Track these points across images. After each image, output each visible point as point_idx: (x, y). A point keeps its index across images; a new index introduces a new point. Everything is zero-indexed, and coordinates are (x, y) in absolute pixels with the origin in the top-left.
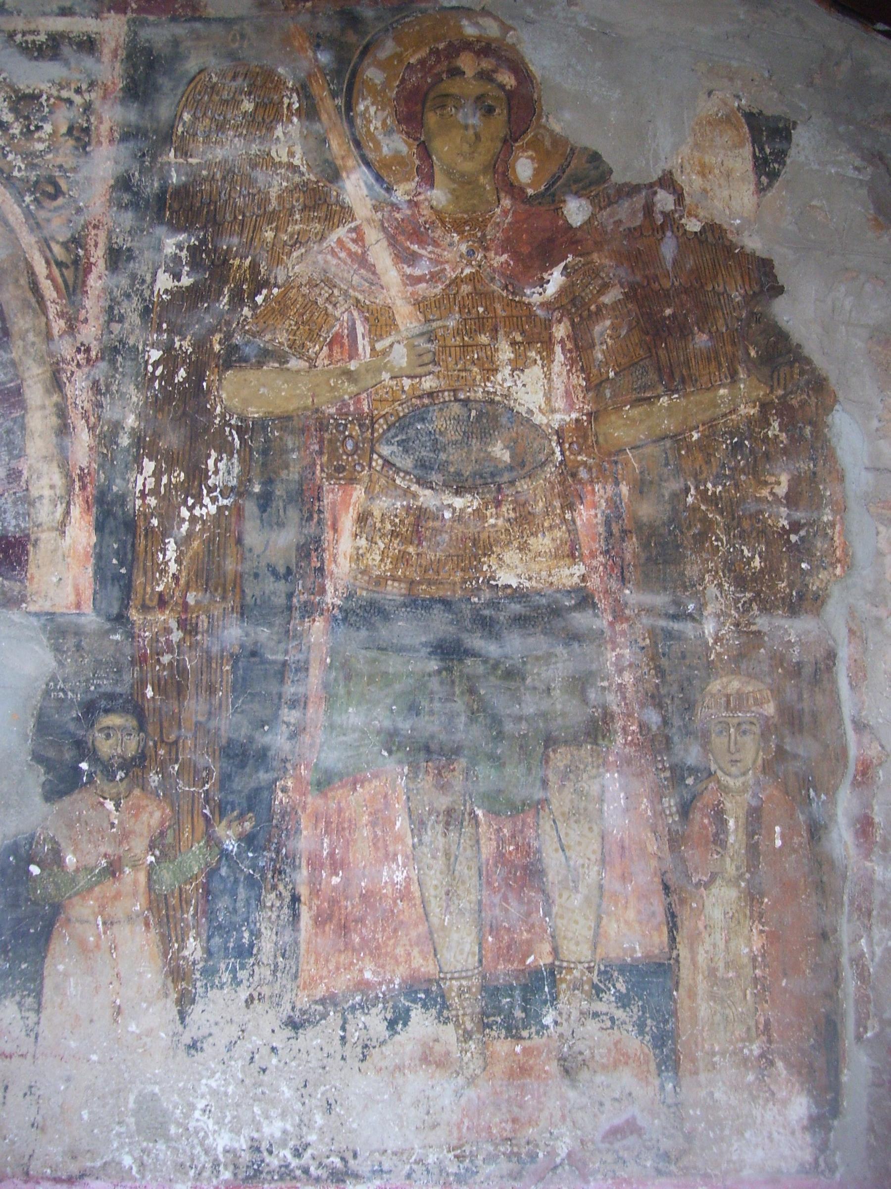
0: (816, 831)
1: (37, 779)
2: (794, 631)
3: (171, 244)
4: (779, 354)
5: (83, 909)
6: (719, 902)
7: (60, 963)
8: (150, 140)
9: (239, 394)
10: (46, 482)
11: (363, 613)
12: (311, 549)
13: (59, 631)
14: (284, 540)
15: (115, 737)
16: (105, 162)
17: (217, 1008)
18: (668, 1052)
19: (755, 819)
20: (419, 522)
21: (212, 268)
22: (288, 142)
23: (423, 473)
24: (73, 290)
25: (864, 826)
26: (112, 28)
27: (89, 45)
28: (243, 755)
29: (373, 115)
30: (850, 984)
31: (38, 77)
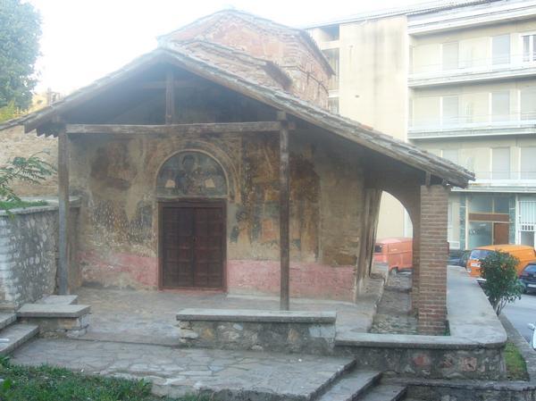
0: (316, 226)
1: (236, 220)
2: (315, 205)
3: (248, 164)
4: (314, 174)
5: (241, 233)
6: (306, 233)
7: (239, 238)
8: (244, 152)
9: (255, 180)
10: (236, 191)
11: (268, 203)
12: (263, 197)
13: (238, 205)
14: (260, 196)
15: (244, 216)
16: (240, 154)
17: (254, 243)
18: (300, 249)
19: (310, 225)
20: (274, 194)
21: (252, 167)
22: (259, 152)
23: (274, 188)
24: (238, 170)
25: (322, 226)
26: (240, 139)
27: (237, 141)
28: (256, 218)
29: (269, 149)
30: (320, 243)
31: (232, 145)
